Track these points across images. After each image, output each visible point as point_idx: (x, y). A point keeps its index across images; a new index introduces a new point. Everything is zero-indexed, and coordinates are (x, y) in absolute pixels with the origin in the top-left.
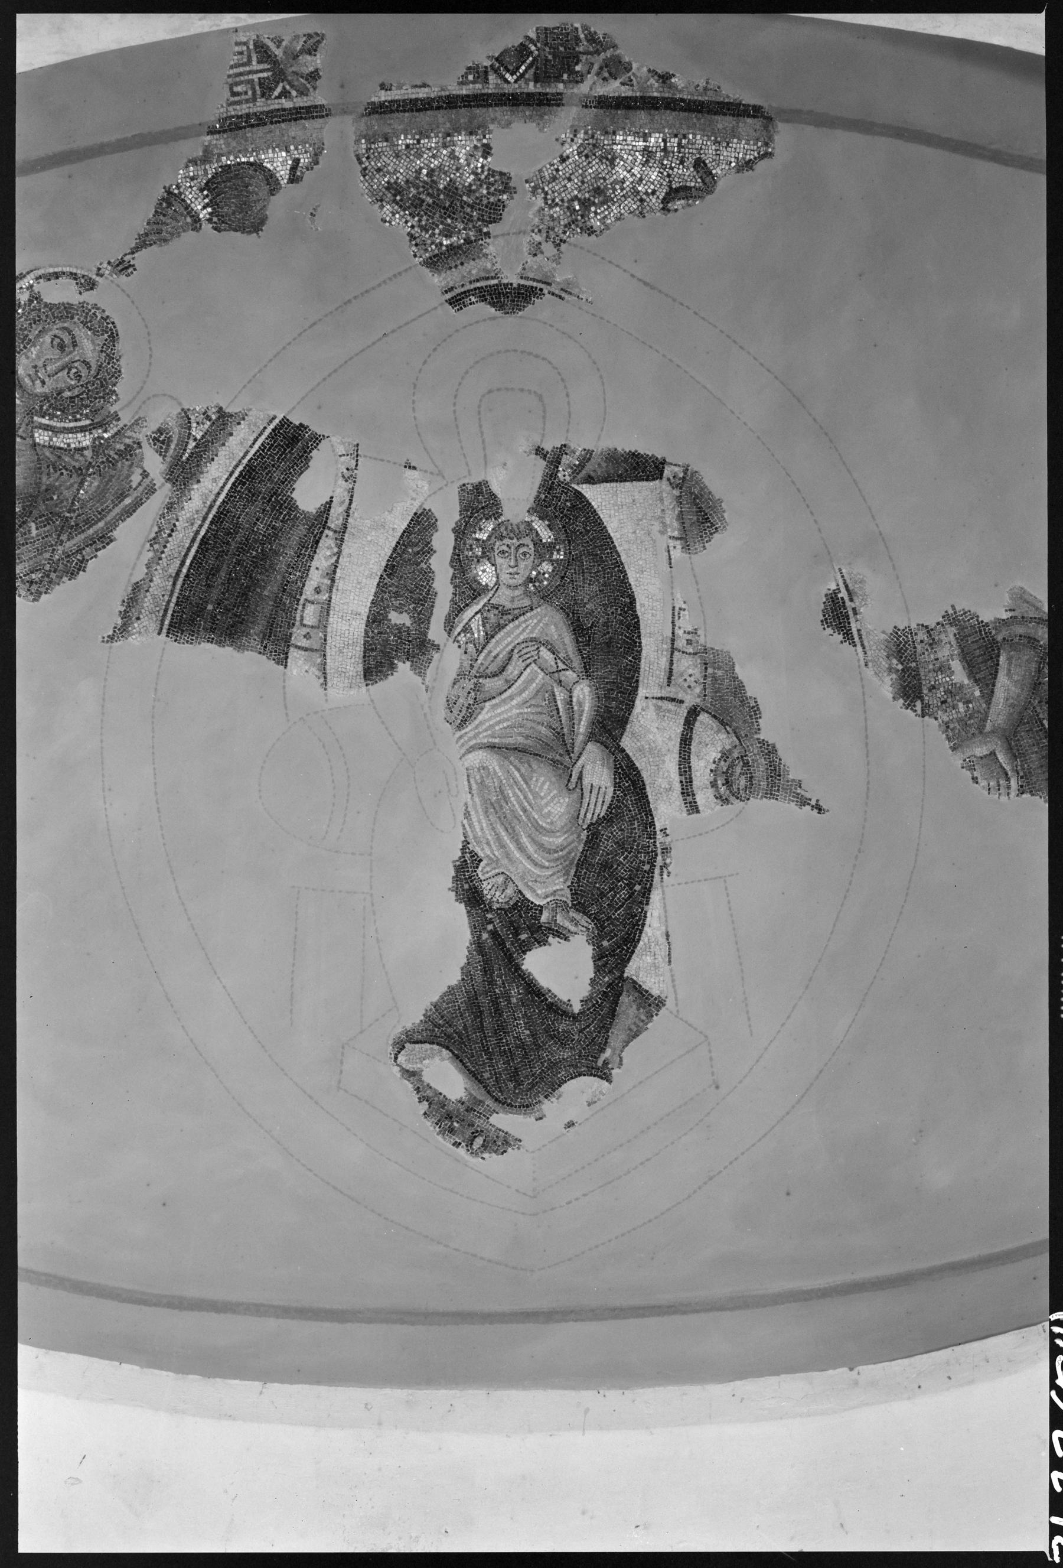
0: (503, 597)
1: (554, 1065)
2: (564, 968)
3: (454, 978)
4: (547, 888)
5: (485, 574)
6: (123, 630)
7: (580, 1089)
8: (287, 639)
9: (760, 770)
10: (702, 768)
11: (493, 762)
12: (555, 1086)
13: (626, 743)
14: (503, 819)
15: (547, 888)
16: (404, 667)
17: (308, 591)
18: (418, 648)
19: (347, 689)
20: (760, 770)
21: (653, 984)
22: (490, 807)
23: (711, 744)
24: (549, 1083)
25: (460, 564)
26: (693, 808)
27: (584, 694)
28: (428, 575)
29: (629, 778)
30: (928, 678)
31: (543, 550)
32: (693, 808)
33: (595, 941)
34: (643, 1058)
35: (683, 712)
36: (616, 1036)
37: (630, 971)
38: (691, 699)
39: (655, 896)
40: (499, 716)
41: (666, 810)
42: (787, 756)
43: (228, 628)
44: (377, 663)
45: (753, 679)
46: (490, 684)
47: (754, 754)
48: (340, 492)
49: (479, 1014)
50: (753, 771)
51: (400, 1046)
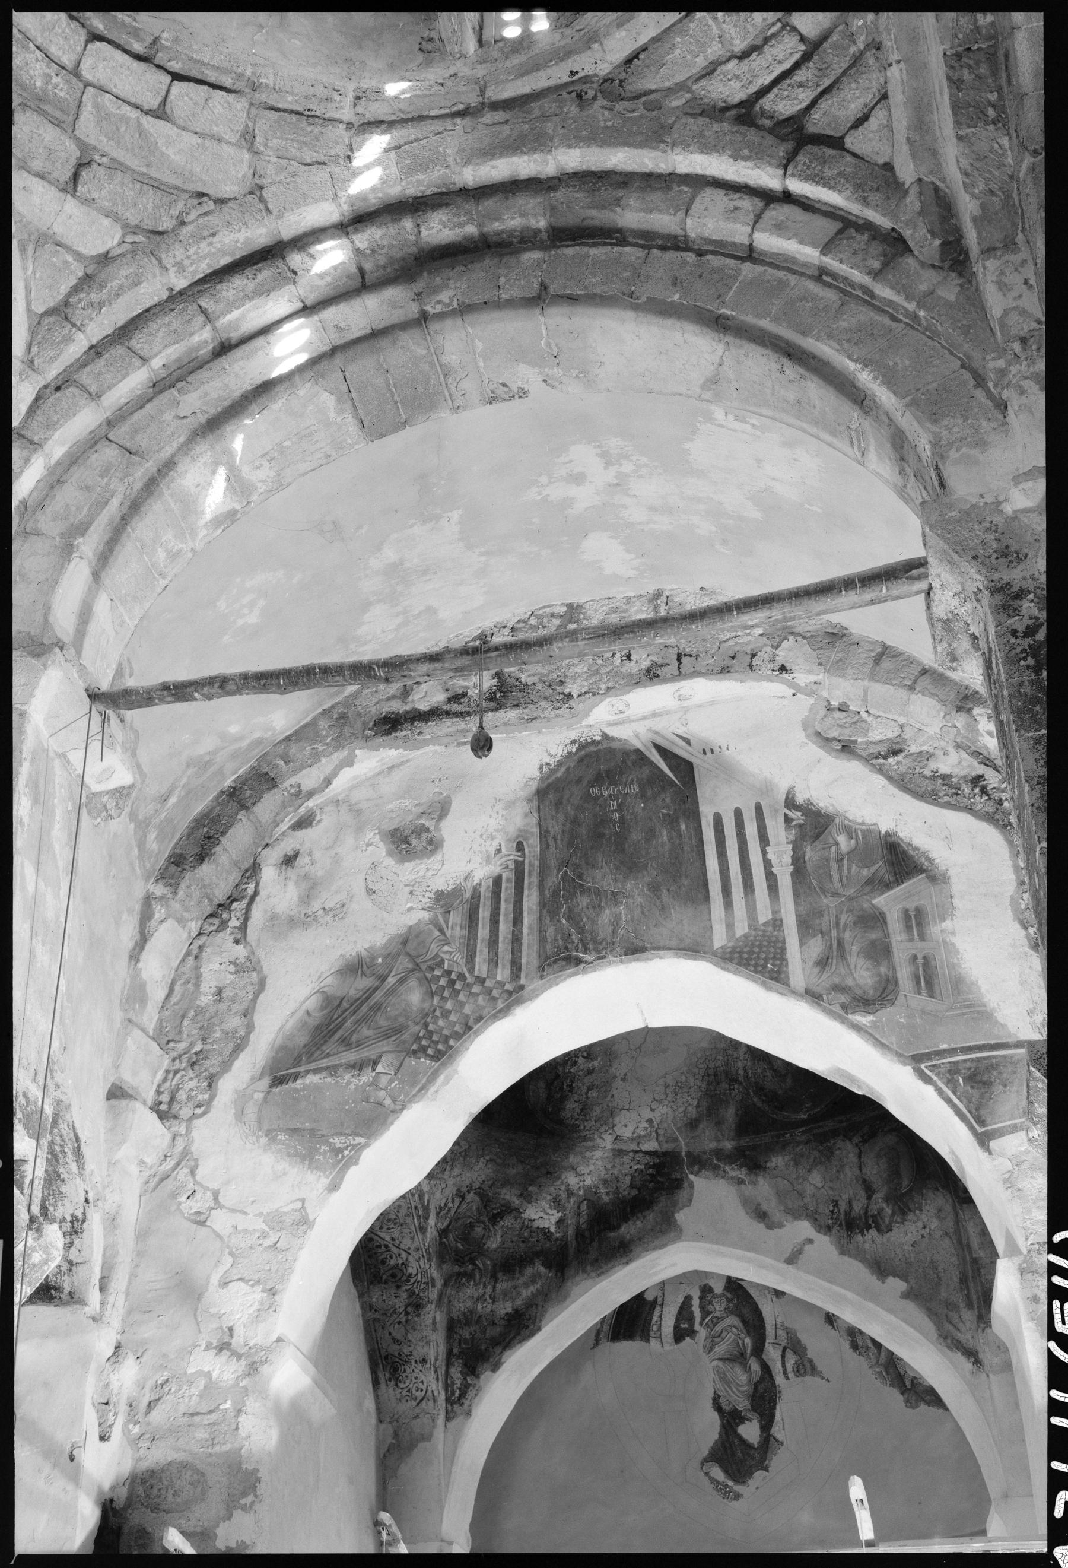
0: (717, 1314)
1: (751, 1466)
2: (750, 1431)
3: (716, 1437)
4: (742, 1404)
5: (711, 1308)
6: (597, 1342)
7: (759, 1474)
8: (649, 1335)
9: (808, 1366)
10: (790, 1365)
11: (720, 1364)
12: (751, 1474)
13: (764, 1357)
14: (726, 1383)
15: (742, 1404)
16: (688, 1339)
17: (653, 1321)
18: (692, 1333)
19: (669, 1346)
20: (808, 1366)
21: (779, 1437)
22: (721, 1378)
23: (791, 1360)
24: (750, 1474)
25: (702, 1307)
26: (788, 1379)
27: (748, 1341)
28: (692, 1313)
29: (766, 1369)
30: (860, 1343)
31: (729, 1301)
32: (788, 1379)
33: (760, 1422)
34: (778, 1461)
35: (781, 1348)
36: (769, 1455)
37: (772, 1432)
38: (784, 1344)
39: (778, 1407)
40: (721, 1349)
41: (779, 1379)
42: (816, 1362)
43: (629, 1336)
44: (679, 1336)
45: (804, 1338)
46: (716, 1340)
47: (806, 1362)
48: (660, 1294)
49: (725, 1450)
50: (805, 1367)
51: (702, 1464)
